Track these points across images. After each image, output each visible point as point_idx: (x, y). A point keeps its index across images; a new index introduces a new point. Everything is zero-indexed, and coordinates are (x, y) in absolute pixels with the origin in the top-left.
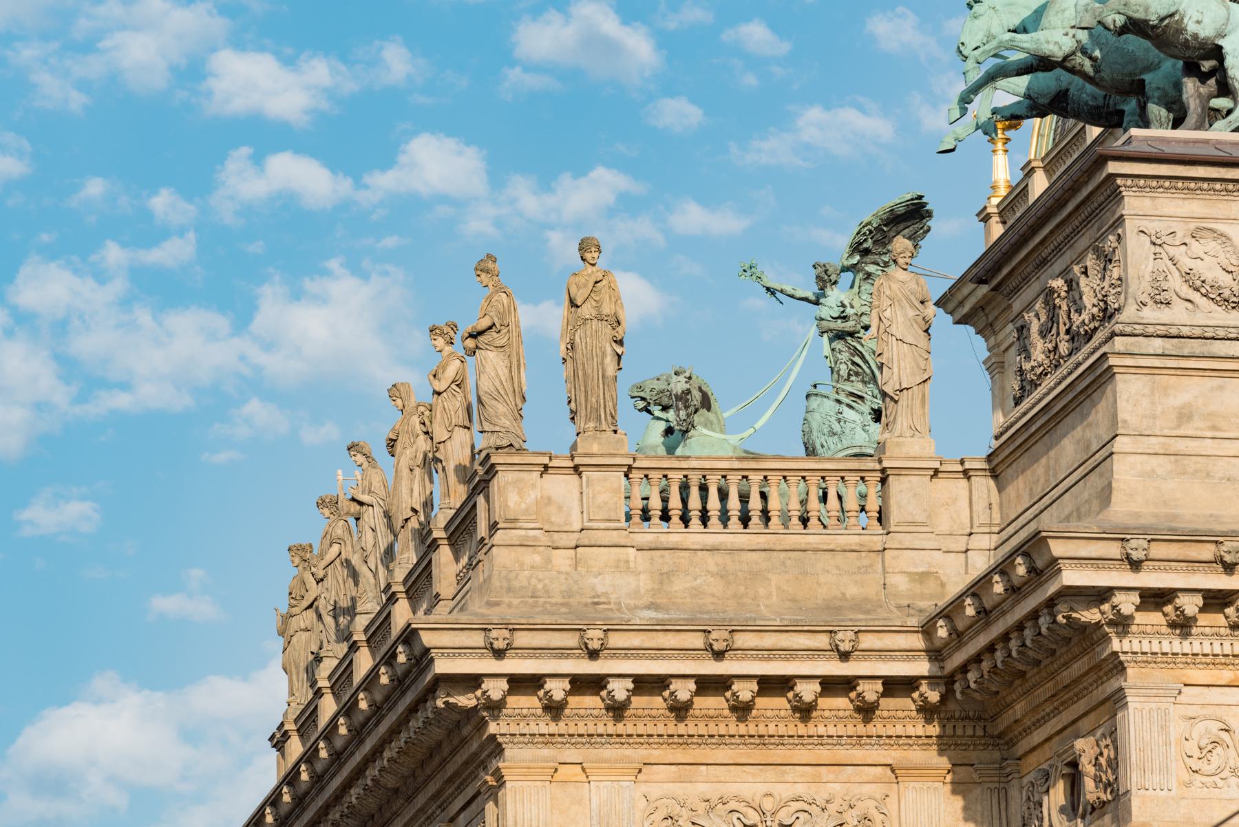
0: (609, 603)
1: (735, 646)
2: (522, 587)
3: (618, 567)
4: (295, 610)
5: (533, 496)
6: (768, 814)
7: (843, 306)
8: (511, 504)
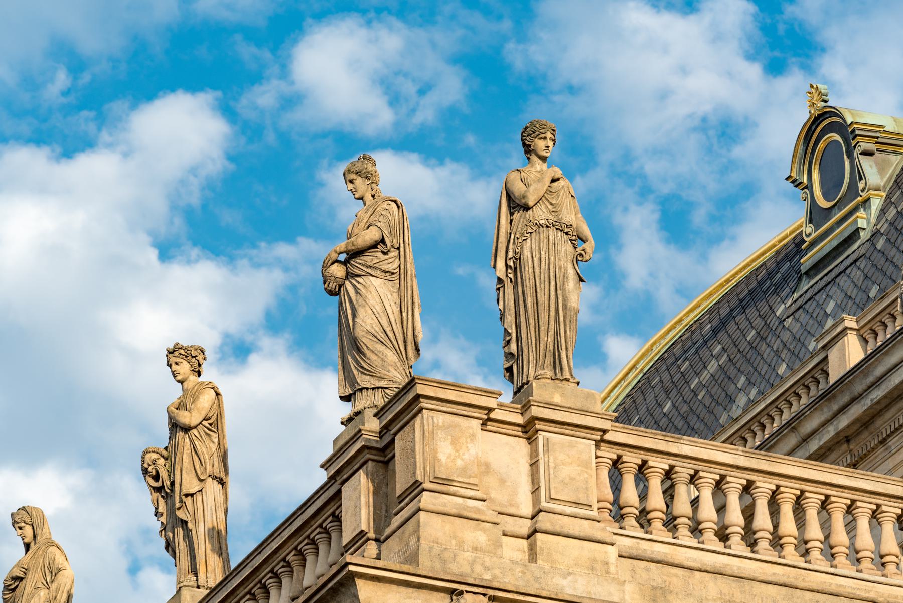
3: (593, 569)
5: (473, 451)
8: (442, 456)
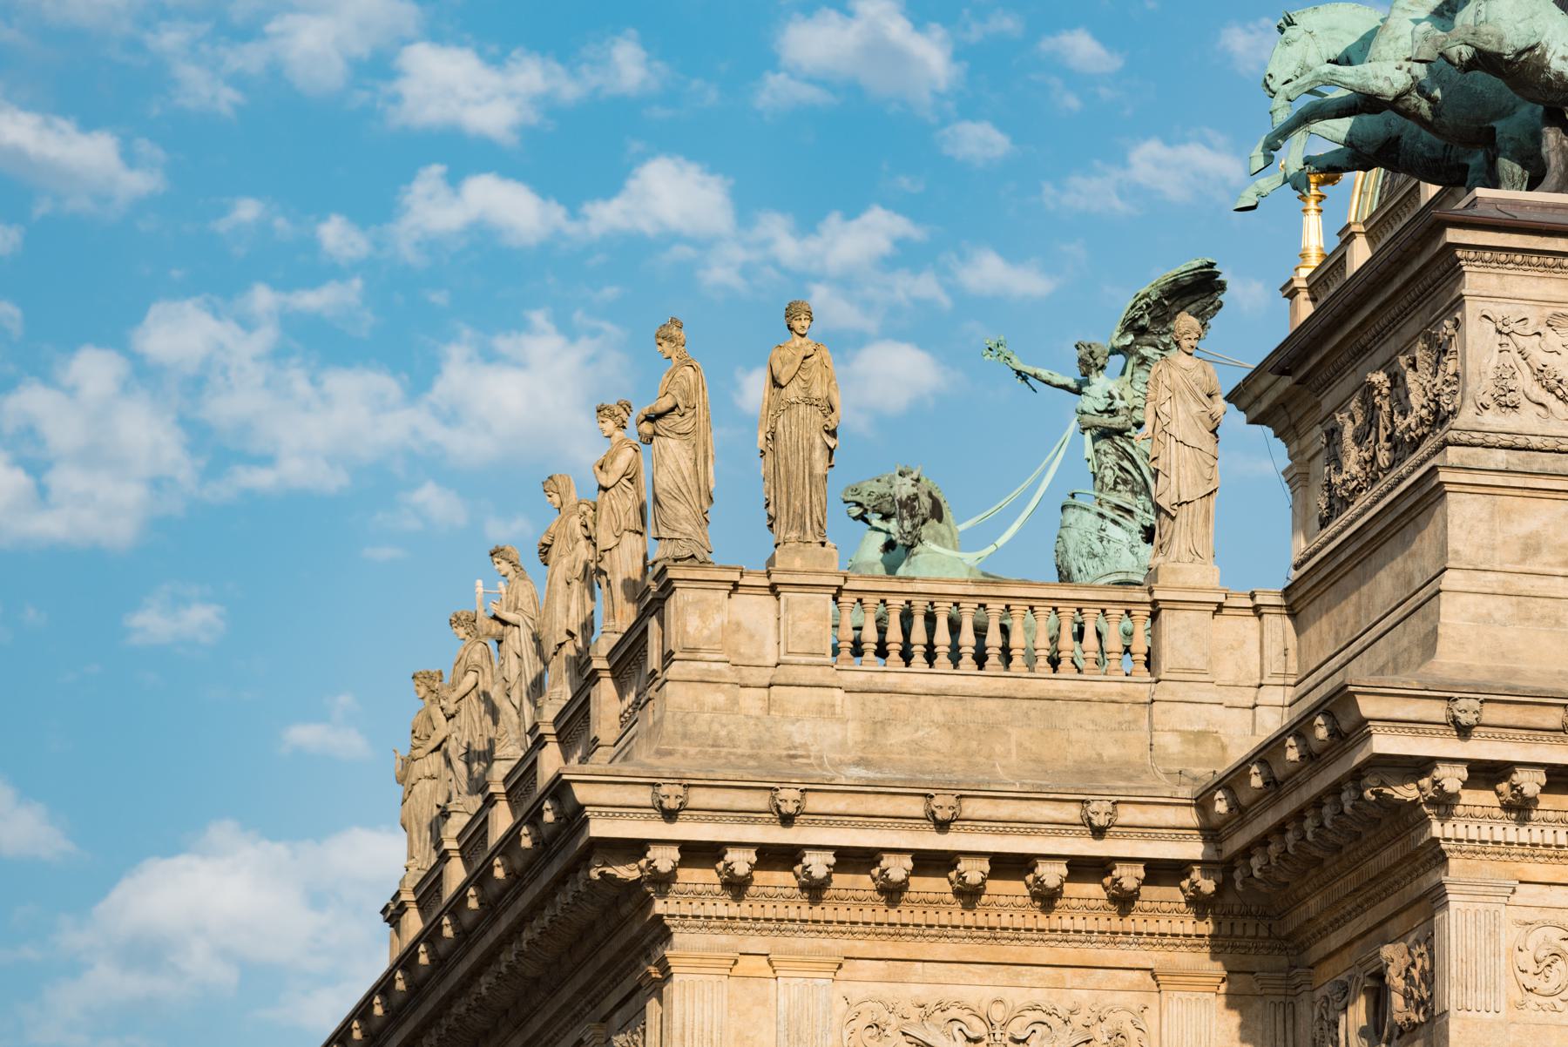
0: (808, 757)
1: (963, 815)
2: (701, 734)
4: (417, 753)
5: (718, 621)
6: (998, 1025)
7: (1111, 397)
8: (690, 629)
